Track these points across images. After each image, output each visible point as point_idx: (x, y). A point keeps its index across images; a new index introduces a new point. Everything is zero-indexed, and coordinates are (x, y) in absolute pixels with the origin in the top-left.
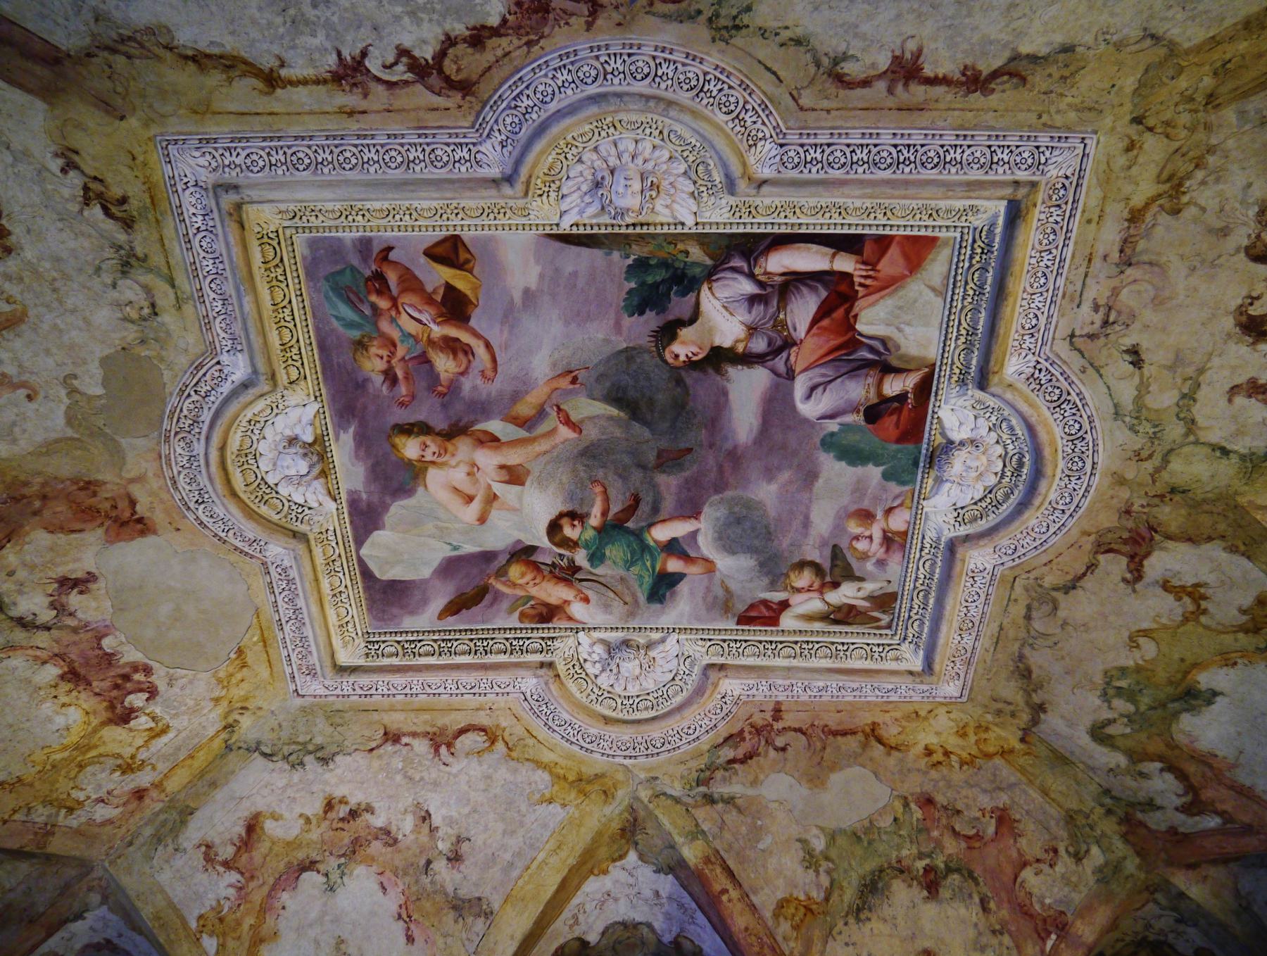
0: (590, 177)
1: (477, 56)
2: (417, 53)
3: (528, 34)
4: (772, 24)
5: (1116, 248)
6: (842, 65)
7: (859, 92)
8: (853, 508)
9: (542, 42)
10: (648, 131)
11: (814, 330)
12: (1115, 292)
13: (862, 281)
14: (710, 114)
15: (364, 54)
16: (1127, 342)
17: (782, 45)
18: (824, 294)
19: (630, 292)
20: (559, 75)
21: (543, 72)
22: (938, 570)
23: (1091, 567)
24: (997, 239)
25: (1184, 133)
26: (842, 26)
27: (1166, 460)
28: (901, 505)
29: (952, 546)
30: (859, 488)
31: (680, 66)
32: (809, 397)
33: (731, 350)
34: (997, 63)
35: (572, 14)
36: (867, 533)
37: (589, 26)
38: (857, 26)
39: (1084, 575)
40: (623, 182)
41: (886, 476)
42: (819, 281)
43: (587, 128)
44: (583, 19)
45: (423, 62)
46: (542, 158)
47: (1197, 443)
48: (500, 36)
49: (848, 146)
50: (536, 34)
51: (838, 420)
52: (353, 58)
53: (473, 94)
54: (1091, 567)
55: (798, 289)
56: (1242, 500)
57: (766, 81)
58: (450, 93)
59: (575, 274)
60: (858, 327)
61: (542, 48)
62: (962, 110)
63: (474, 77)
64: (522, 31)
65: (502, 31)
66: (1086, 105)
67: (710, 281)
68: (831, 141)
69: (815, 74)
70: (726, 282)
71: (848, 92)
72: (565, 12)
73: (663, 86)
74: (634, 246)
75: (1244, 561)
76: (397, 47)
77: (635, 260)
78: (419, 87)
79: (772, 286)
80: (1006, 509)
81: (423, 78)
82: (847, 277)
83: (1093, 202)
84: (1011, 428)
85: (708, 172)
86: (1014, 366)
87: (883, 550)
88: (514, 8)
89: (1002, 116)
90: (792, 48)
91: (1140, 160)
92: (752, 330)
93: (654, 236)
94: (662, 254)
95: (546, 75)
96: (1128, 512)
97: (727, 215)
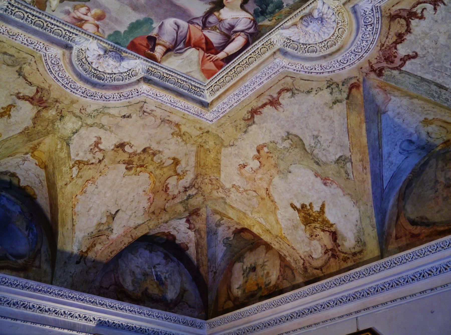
1: (396, 31)
2: (417, 20)
3: (386, 48)
4: (321, 93)
5: (170, 119)
6: (291, 94)
7: (278, 90)
8: (107, 15)
9: (379, 48)
11: (203, 36)
12: (155, 116)
13: (210, 57)
15: (435, 9)
16: (134, 116)
17: (312, 89)
18: (215, 45)
20: (366, 44)
22: (56, 36)
23: (31, 84)
24: (198, 97)
25: (195, 139)
26: (303, 103)
27: (77, 117)
28: (98, 31)
29: (68, 47)
30: (117, 21)
32: (176, 24)
33: (218, 11)
34: (256, 119)
35: (377, 63)
36: (89, 14)
37: (370, 62)
38: (299, 105)
39: (26, 80)
41: (117, 33)
42: (222, 46)
45: (413, 18)
46: (348, 17)
47: (82, 126)
48: (394, 43)
50: (383, 50)
51: (157, 28)
52: (438, 5)
53: (388, 17)
54: (31, 84)
56: (51, 136)
58: (396, 12)
60: (194, 49)
61: (378, 46)
62: (248, 104)
63: (392, 23)
64: (388, 48)
65: (394, 45)
66: (223, 125)
70: (247, 24)
74: (289, 9)
75: (20, 131)
76: (425, 18)
77: (284, 6)
78: (408, 8)
79: (232, 34)
80: (80, 69)
81: (409, 12)
82: (217, 53)
83: (189, 117)
84: (118, 80)
86: (144, 87)
87: (76, 16)
88: (396, 54)
89: (237, 110)
90: (308, 89)
91: (195, 130)
92: (220, 21)
93: (286, 17)
94: (276, 14)
96: (57, 101)
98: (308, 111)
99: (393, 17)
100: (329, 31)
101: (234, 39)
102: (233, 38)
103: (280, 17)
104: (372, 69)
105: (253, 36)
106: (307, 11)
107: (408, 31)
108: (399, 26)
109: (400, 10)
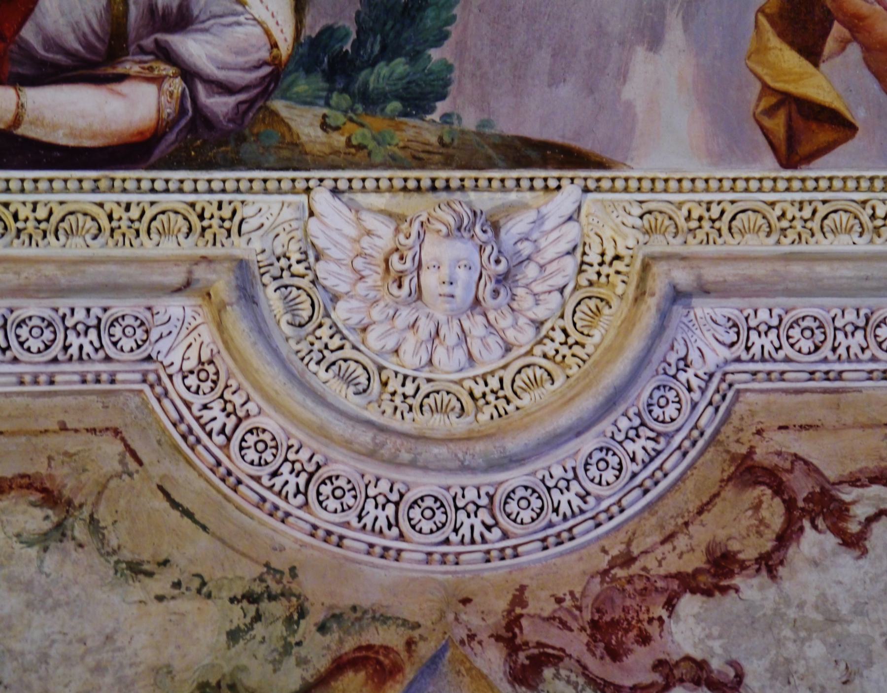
0: (520, 292)
1: (721, 535)
2: (831, 541)
3: (630, 580)
4: (187, 605)
6: (47, 526)
9: (603, 562)
10: (410, 389)
14: (293, 430)
17: (165, 563)
18: (28, 33)
19: (440, 38)
20: (576, 502)
21: (604, 505)
26: (57, 605)
31: (354, 522)
35: (551, 619)
37: (519, 598)
38: (29, 605)
40: (458, 291)
43: (526, 400)
44: (531, 609)
45: (820, 522)
46: (614, 337)
49: (15, 360)
50: (614, 579)
53: (733, 458)
55: (88, 46)
57: (191, 488)
58: (776, 460)
59: (554, 81)
61: (605, 551)
63: (729, 492)
64: (639, 585)
65: (675, 585)
67: (274, 61)
68: (53, 368)
69: (96, 504)
70: (241, 60)
71: (31, 471)
72: (564, 625)
73: (384, 486)
74: (434, 140)
76: (865, 552)
77: (432, 110)
78: (832, 473)
79: (142, 51)
81: (824, 492)
85: (291, 307)
88: (653, 630)
90: (146, 556)
94: (376, 122)
95: (599, 499)
97: (247, 211)
98: (44, 658)
99: (751, 469)
100: (486, 346)
101: (122, 78)
102: (130, 67)
103: (371, 145)
104: (508, 636)
105: (193, 140)
106: (484, 201)
107: (769, 564)
108: (747, 520)
109: (796, 457)
